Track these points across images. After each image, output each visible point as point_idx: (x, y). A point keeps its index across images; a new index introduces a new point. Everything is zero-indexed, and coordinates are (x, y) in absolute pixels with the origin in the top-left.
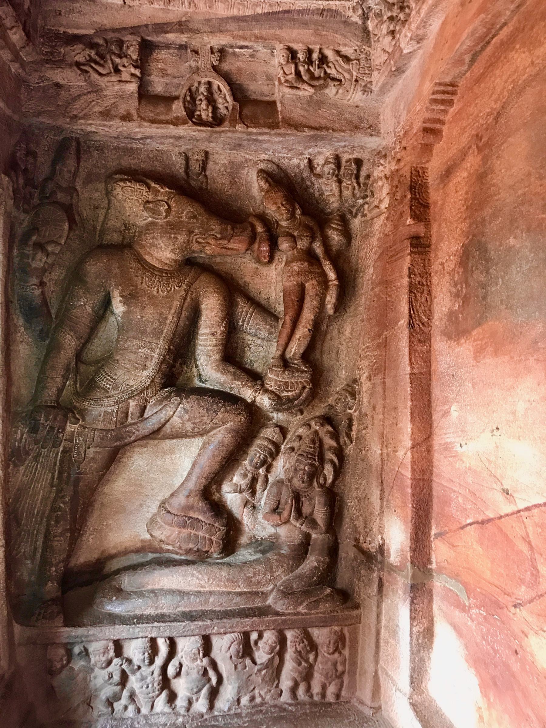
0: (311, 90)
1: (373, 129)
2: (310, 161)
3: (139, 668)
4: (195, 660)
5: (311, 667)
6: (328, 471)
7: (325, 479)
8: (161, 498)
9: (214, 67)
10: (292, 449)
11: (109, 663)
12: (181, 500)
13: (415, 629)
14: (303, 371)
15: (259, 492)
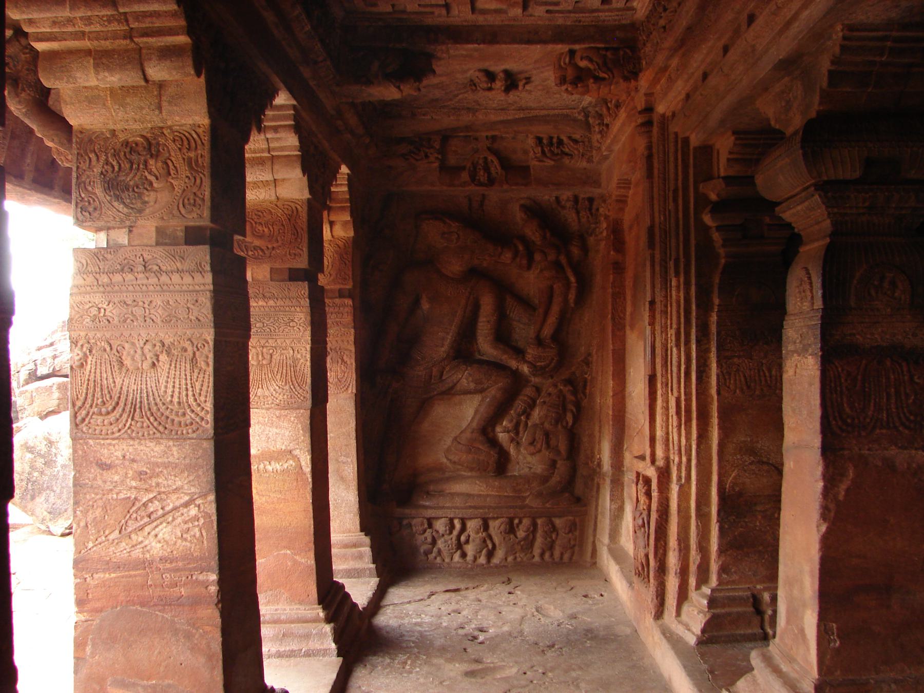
0: (552, 163)
1: (597, 183)
2: (557, 198)
3: (443, 535)
4: (477, 533)
5: (553, 542)
6: (569, 418)
7: (567, 423)
8: (453, 435)
9: (489, 149)
10: (544, 402)
11: (425, 531)
12: (468, 434)
13: (613, 507)
14: (552, 348)
15: (521, 432)
